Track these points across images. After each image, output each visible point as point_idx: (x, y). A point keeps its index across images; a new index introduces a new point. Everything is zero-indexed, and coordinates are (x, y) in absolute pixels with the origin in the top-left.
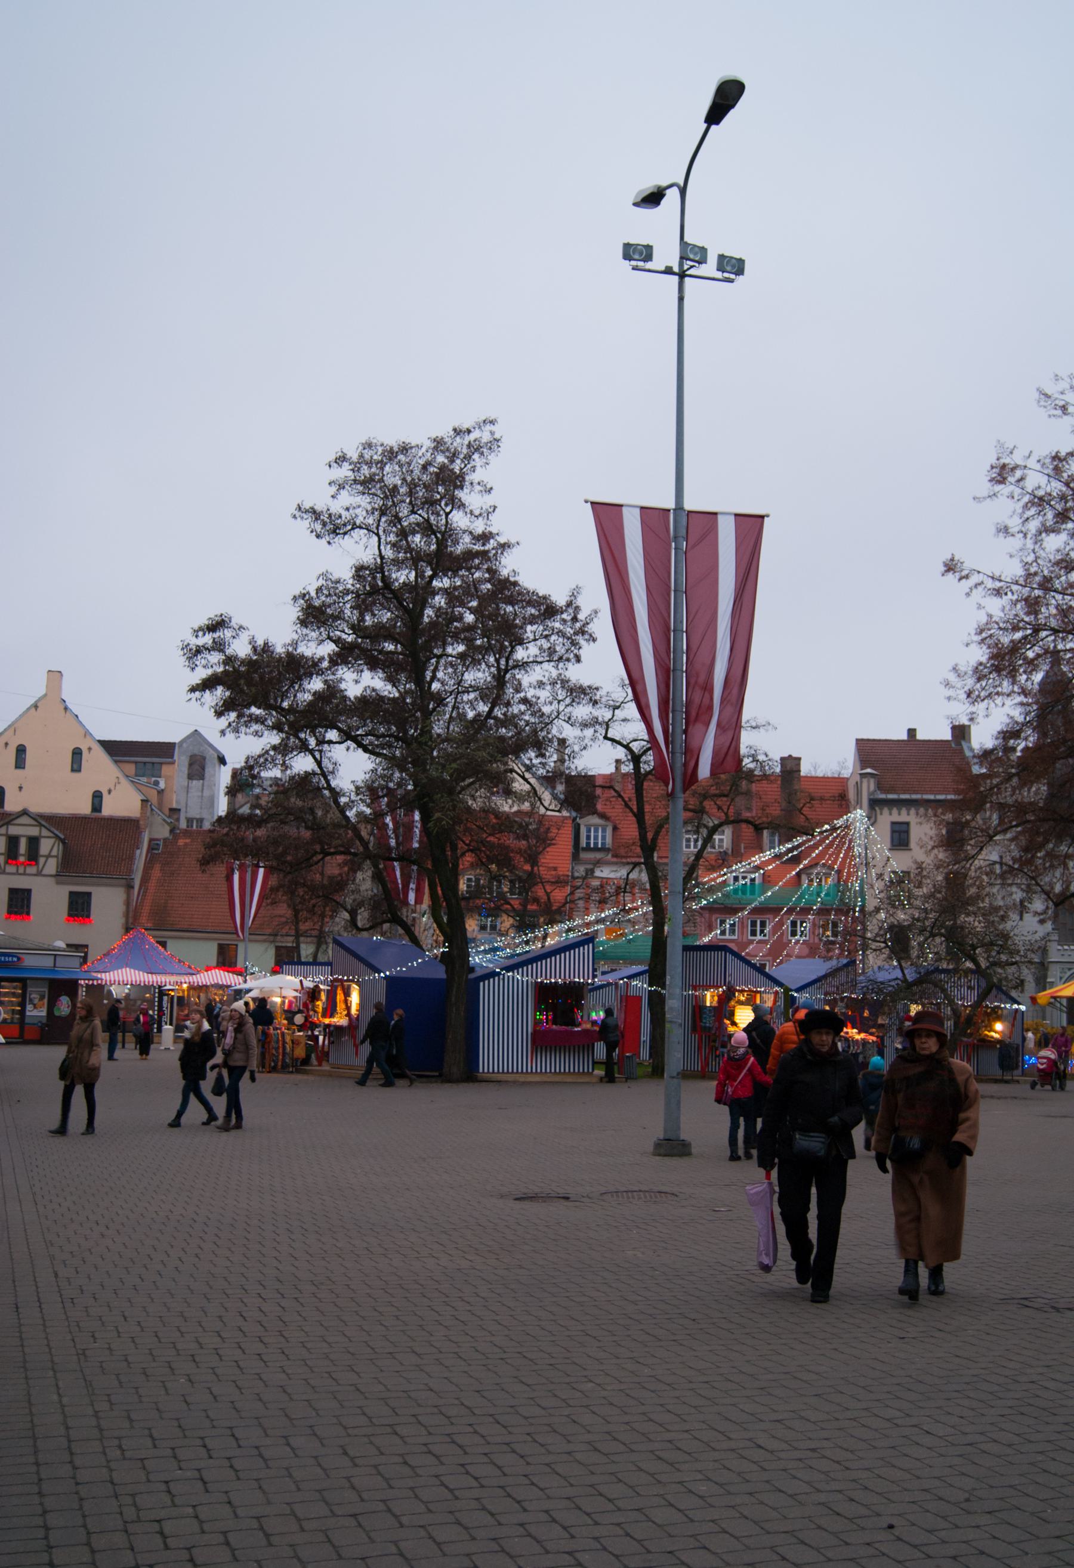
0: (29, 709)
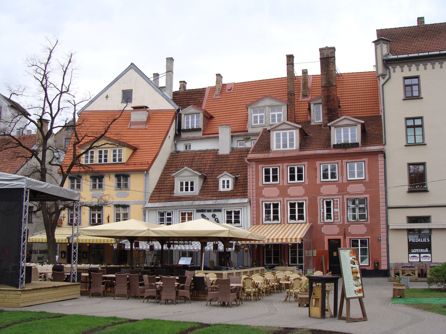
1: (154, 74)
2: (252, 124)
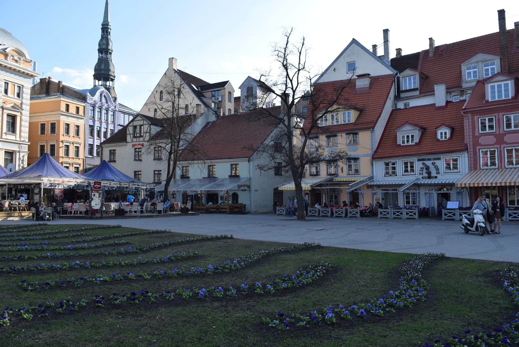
0: (164, 75)
1: (373, 46)
2: (465, 80)
